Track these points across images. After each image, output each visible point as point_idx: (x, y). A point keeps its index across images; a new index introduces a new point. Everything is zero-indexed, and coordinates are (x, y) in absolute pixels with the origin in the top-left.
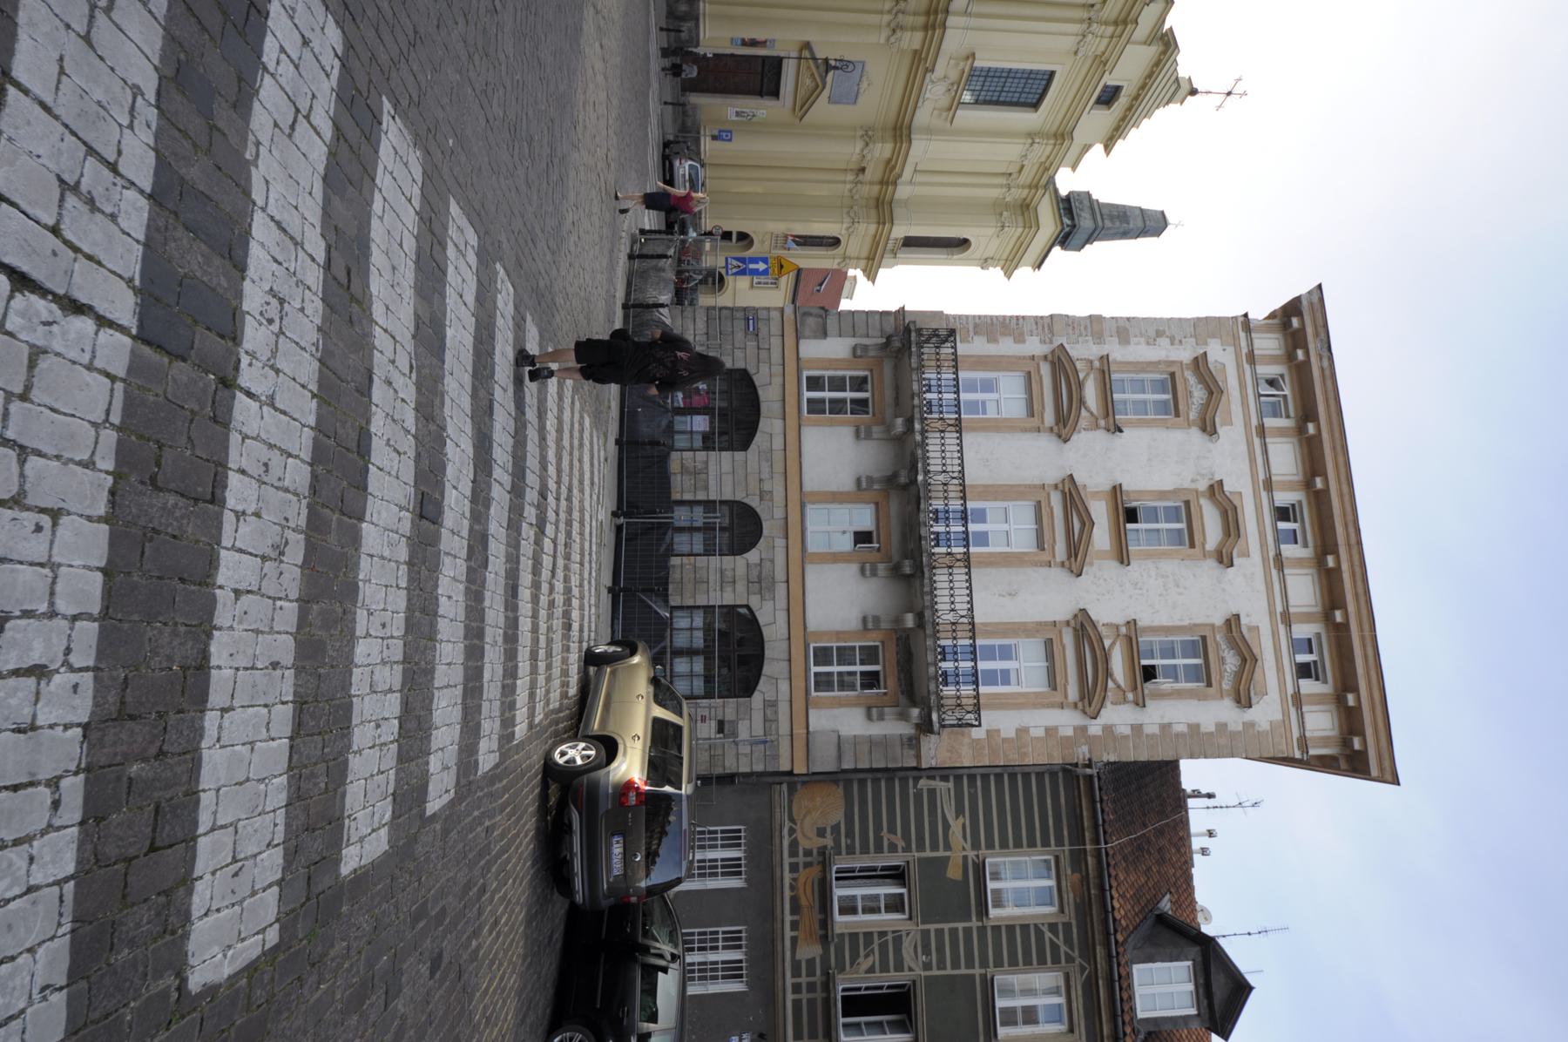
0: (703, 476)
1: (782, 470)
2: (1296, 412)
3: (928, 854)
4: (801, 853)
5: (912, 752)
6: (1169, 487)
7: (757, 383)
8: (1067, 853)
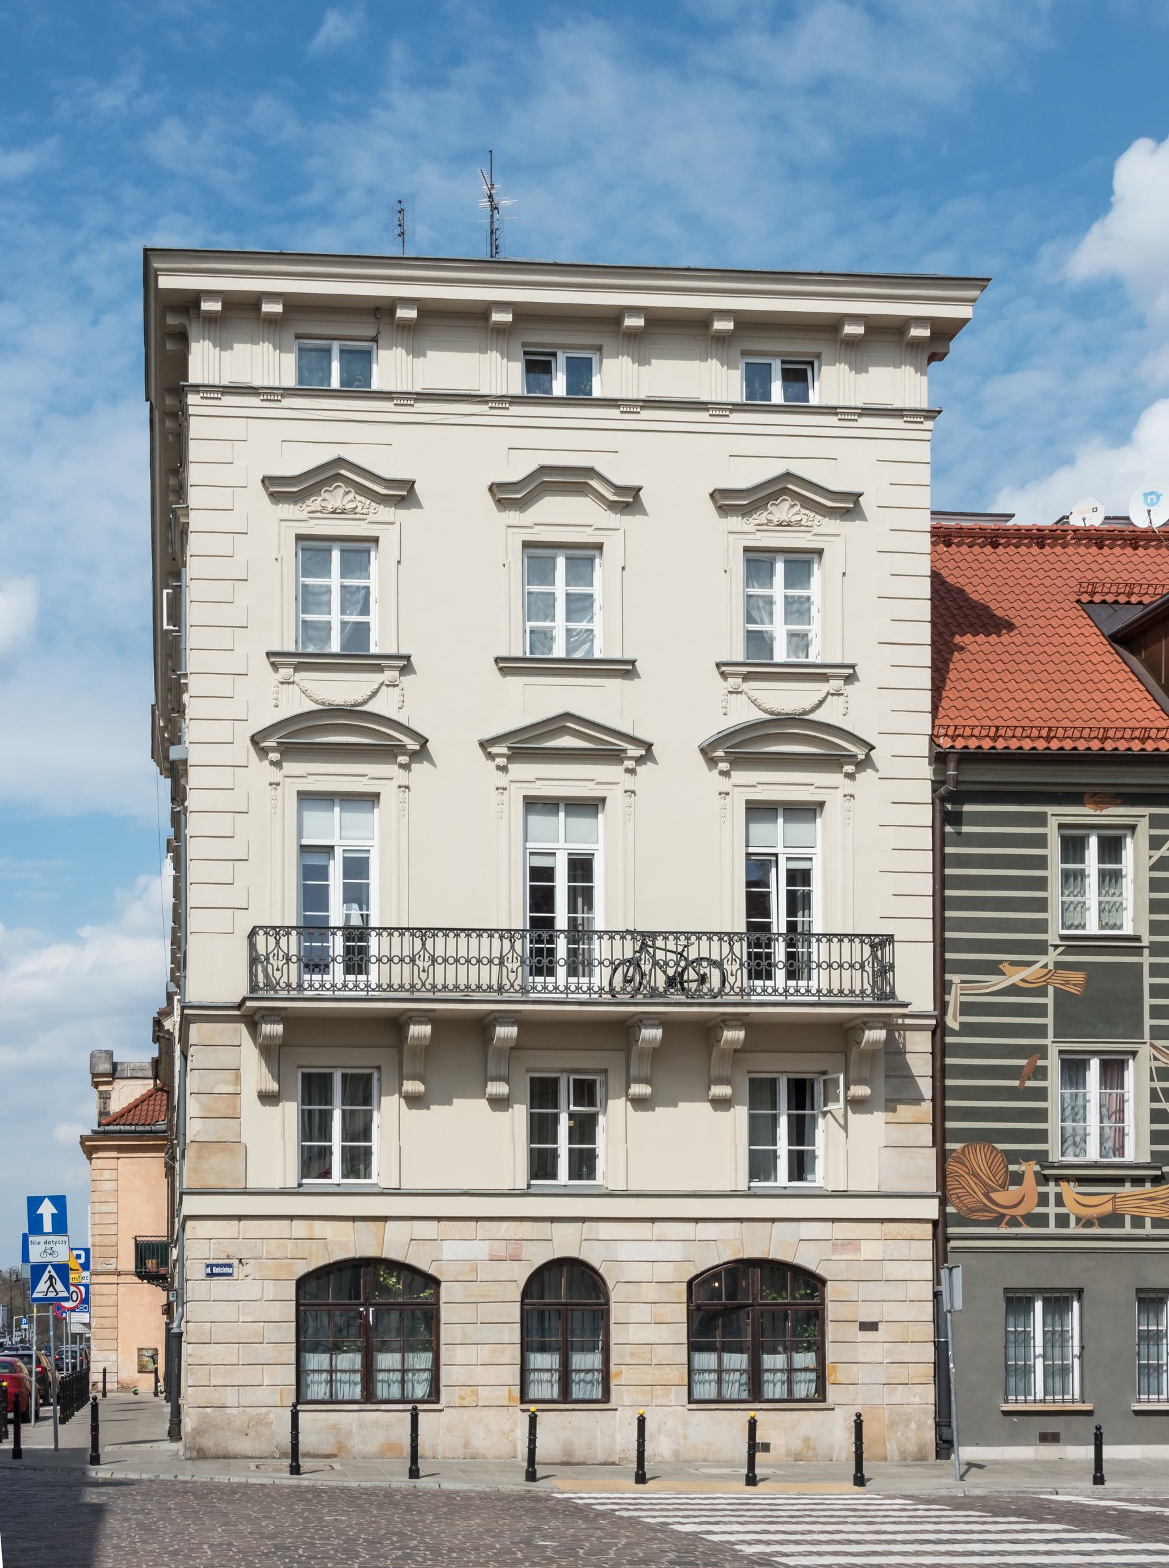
3: (1049, 1021)
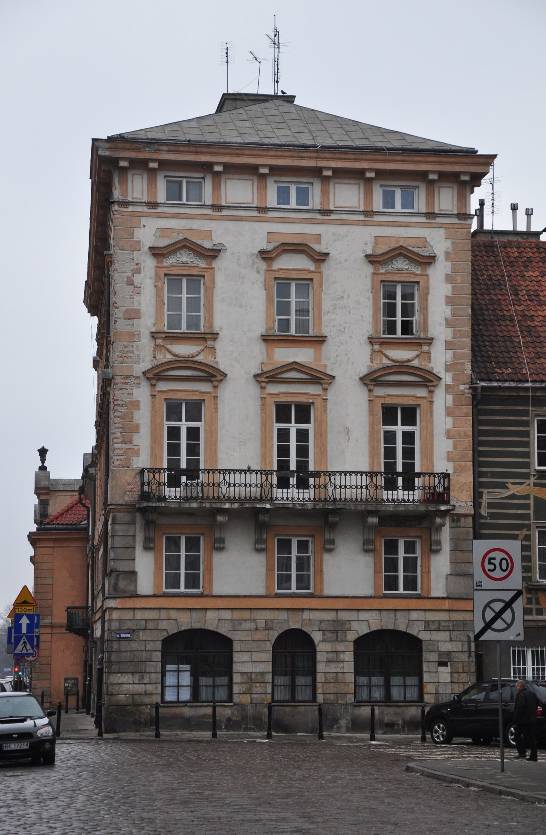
0: (253, 676)
1: (249, 612)
2: (200, 172)
3: (531, 512)
4: (529, 606)
5: (462, 519)
6: (263, 294)
7: (176, 631)
8: (533, 409)
